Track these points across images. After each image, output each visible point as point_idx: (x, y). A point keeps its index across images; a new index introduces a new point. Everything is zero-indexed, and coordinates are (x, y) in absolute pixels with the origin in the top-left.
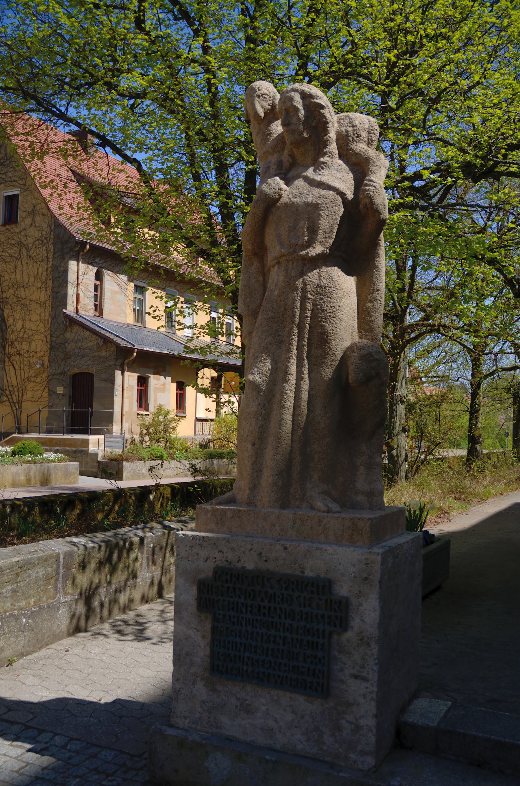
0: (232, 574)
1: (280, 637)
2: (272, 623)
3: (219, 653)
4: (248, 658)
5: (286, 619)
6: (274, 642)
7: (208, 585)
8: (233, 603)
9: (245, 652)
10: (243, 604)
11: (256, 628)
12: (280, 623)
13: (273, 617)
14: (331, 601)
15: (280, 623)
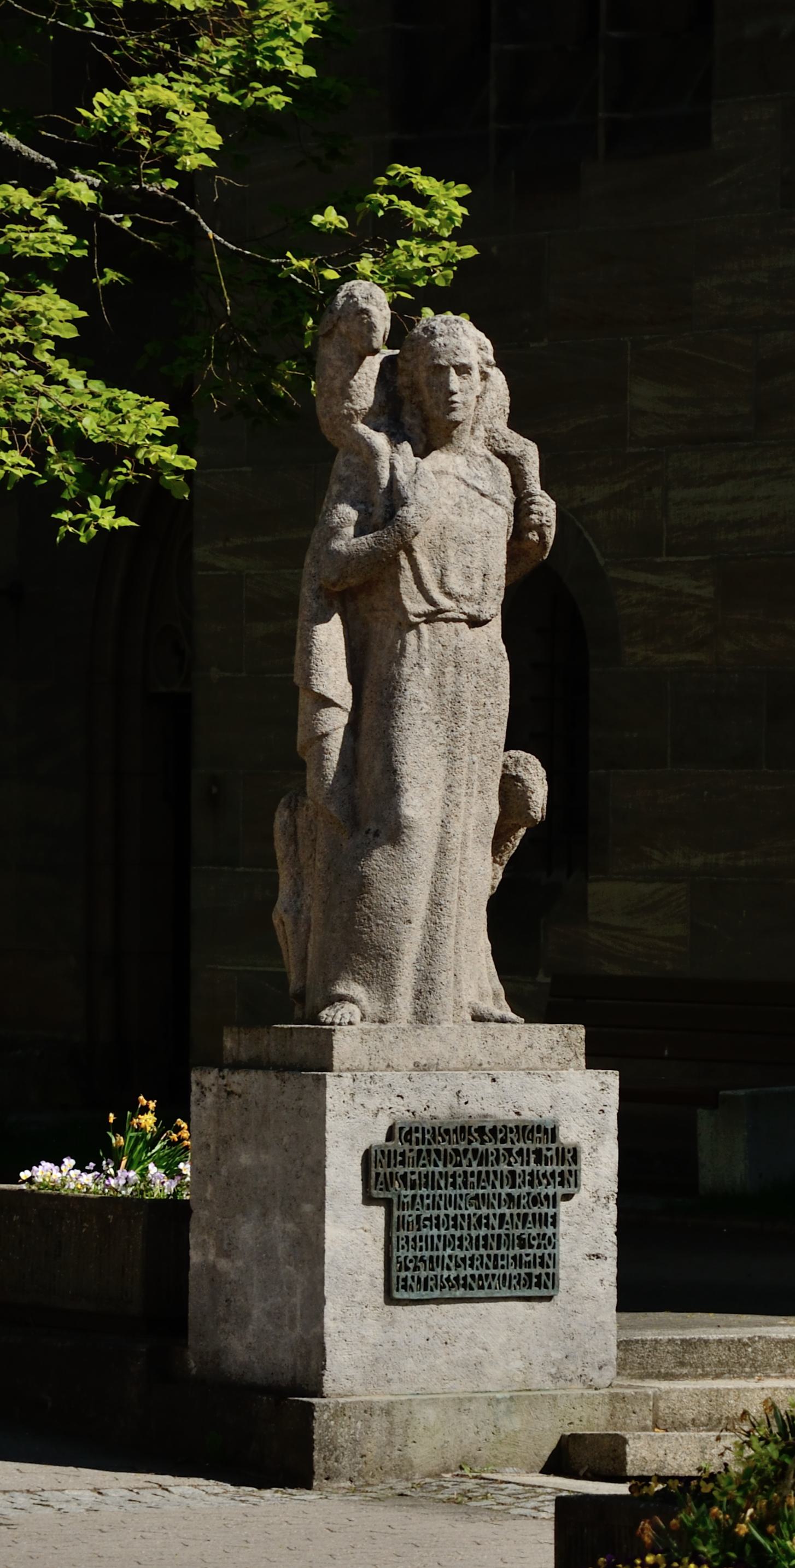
0: (423, 1129)
1: (494, 1215)
2: (483, 1195)
3: (406, 1258)
4: (450, 1257)
5: (502, 1187)
6: (487, 1225)
7: (389, 1151)
8: (426, 1176)
9: (444, 1249)
10: (440, 1173)
11: (460, 1208)
12: (494, 1195)
13: (484, 1188)
14: (563, 1149)
15: (494, 1195)
